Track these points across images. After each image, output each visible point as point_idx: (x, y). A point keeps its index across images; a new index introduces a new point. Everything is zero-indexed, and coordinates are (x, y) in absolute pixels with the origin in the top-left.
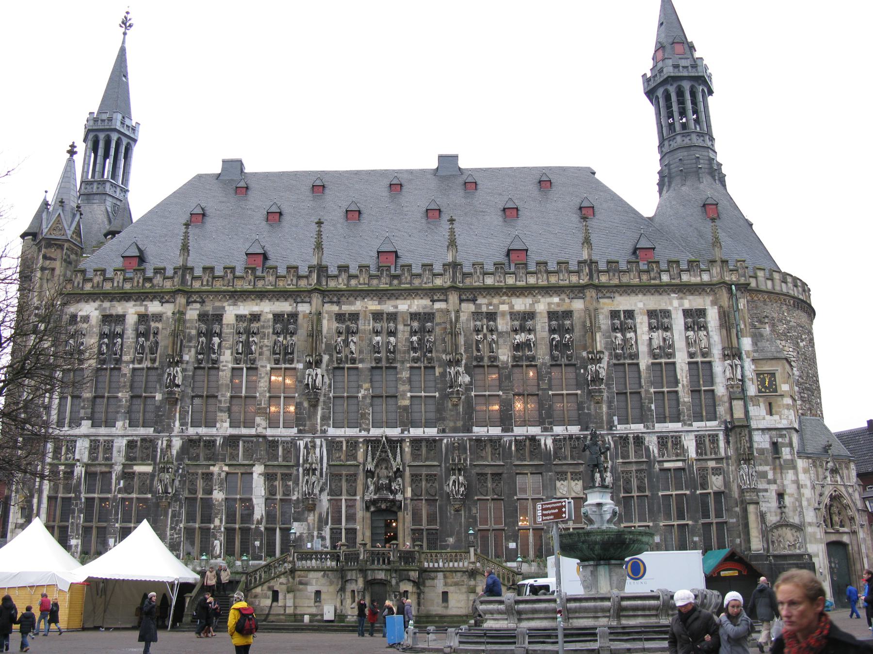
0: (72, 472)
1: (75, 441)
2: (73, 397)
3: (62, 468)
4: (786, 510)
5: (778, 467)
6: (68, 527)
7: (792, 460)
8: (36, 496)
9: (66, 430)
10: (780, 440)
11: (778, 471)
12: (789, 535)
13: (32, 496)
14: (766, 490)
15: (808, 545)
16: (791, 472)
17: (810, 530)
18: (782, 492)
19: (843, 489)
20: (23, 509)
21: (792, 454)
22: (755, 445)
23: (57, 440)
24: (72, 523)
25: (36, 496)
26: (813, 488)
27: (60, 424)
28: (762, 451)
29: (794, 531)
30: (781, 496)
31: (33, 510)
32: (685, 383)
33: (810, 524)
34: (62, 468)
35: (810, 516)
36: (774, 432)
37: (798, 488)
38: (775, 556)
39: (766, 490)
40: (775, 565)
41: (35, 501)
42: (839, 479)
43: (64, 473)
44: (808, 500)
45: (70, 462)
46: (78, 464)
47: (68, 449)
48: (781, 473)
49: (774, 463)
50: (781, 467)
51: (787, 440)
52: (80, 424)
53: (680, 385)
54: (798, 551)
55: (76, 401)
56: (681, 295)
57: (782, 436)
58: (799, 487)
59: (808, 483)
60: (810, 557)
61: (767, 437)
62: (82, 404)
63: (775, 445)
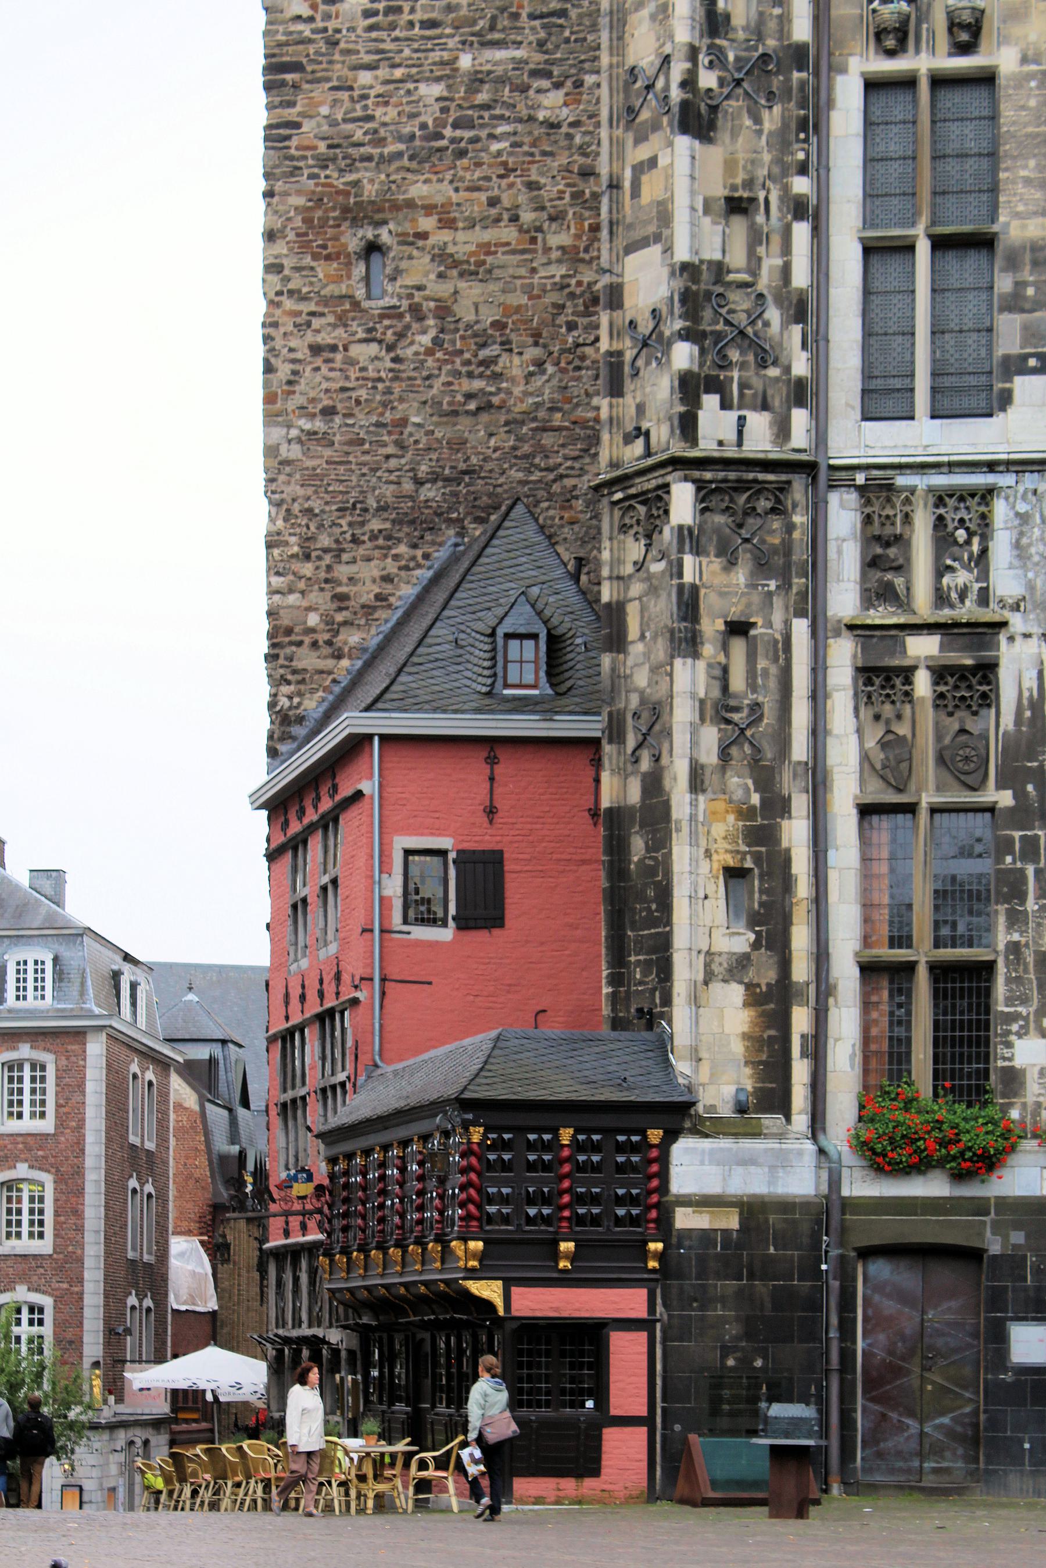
0: (987, 670)
1: (987, 494)
2: (940, 244)
3: (923, 648)
6: (988, 968)
8: (800, 803)
9: (921, 436)
13: (777, 806)
20: (733, 874)
23: (878, 488)
24: (1014, 948)
25: (800, 803)
27: (883, 399)
31: (787, 882)
34: (923, 648)
41: (795, 833)
43: (940, 673)
45: (968, 611)
46: (1017, 622)
47: (943, 539)
52: (1005, 400)
55: (965, 267)
62: (1004, 284)
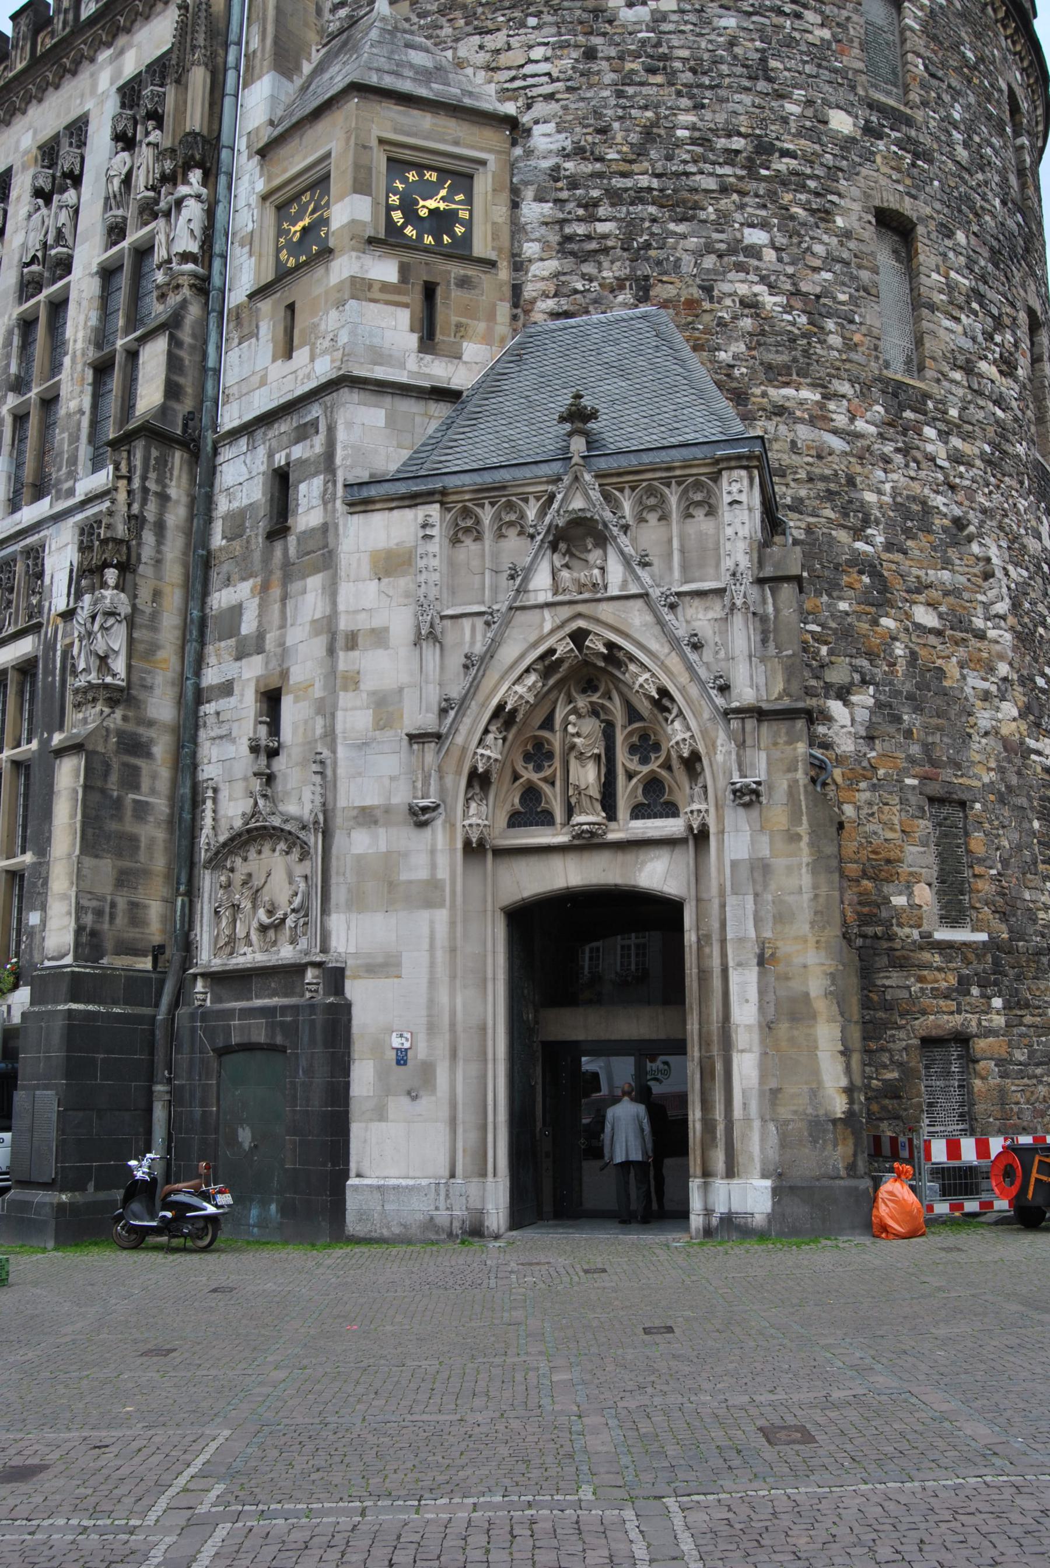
4: (280, 764)
5: (278, 574)
7: (325, 528)
10: (298, 452)
11: (276, 592)
12: (277, 874)
14: (227, 689)
15: (337, 922)
16: (314, 582)
17: (356, 844)
18: (274, 684)
19: (637, 618)
21: (327, 499)
22: (223, 505)
26: (428, 636)
28: (237, 523)
29: (295, 855)
30: (271, 700)
32: (80, 345)
33: (367, 817)
35: (376, 776)
36: (284, 426)
37: (331, 651)
38: (218, 979)
39: (227, 689)
40: (206, 1015)
42: (616, 575)
44: (385, 707)
48: (284, 598)
49: (267, 559)
50: (290, 573)
51: (317, 444)
53: (67, 361)
54: (286, 953)
56: (122, 40)
57: (303, 433)
58: (338, 640)
59: (401, 623)
60: (335, 978)
61: (262, 451)
63: (282, 481)
